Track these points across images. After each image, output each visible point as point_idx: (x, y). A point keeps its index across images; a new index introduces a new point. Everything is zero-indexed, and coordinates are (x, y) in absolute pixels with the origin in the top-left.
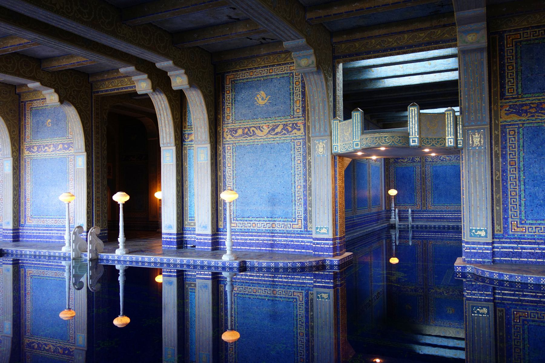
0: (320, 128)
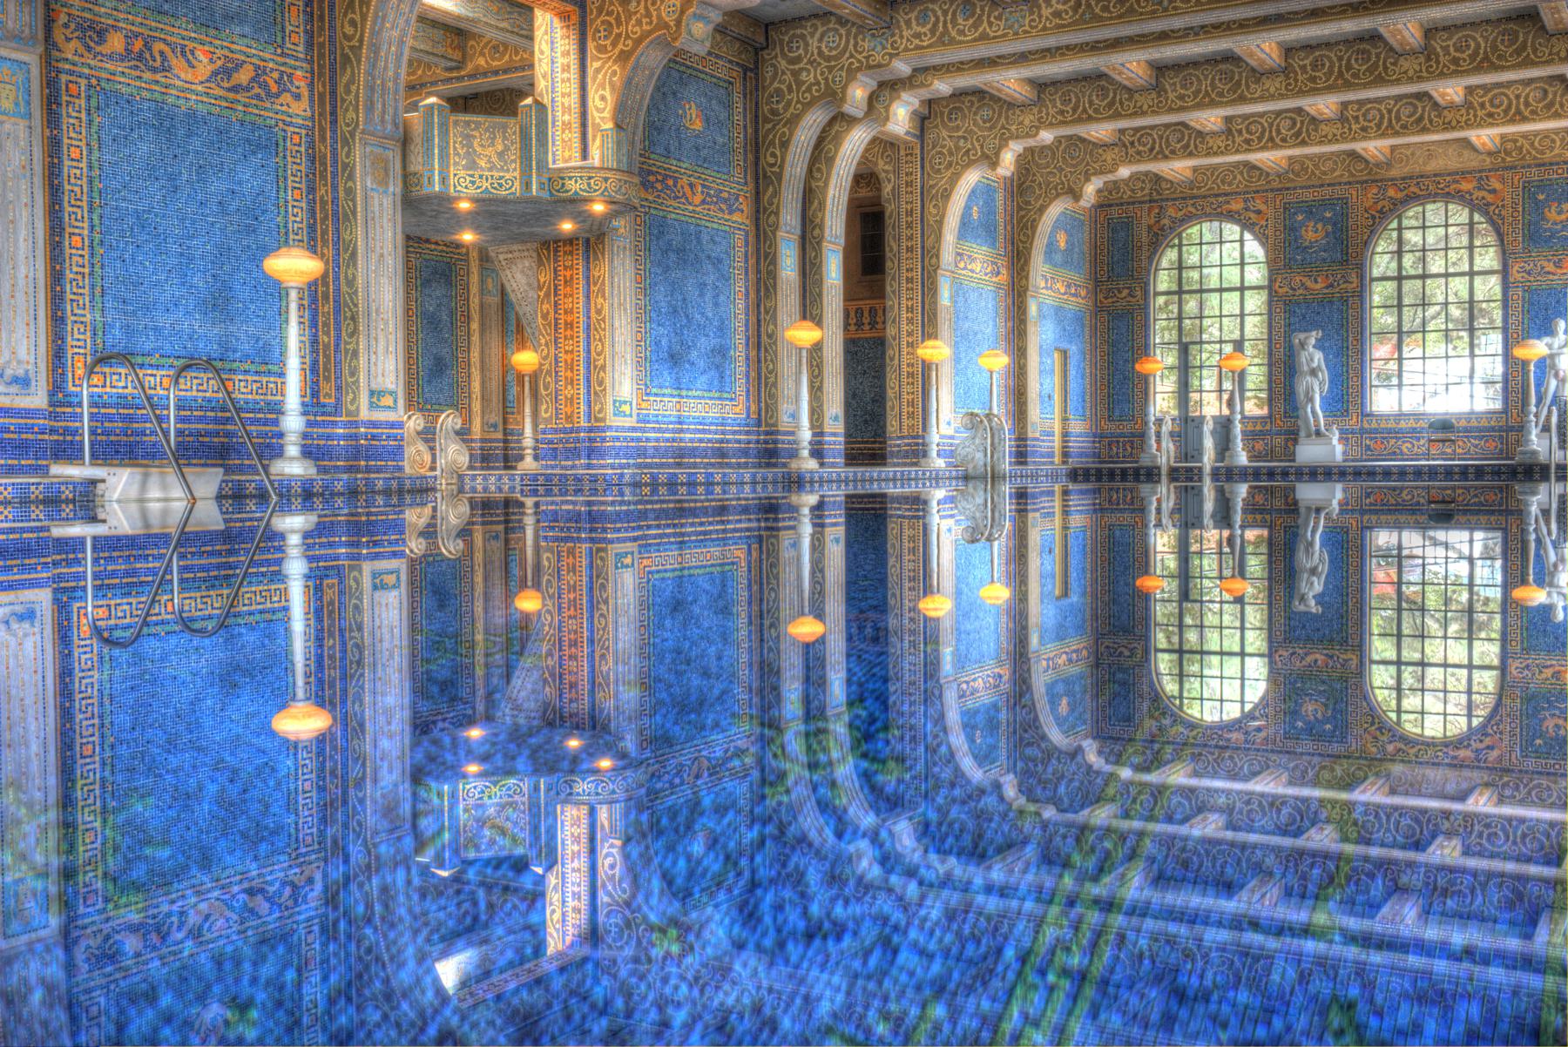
0: (384, 112)
